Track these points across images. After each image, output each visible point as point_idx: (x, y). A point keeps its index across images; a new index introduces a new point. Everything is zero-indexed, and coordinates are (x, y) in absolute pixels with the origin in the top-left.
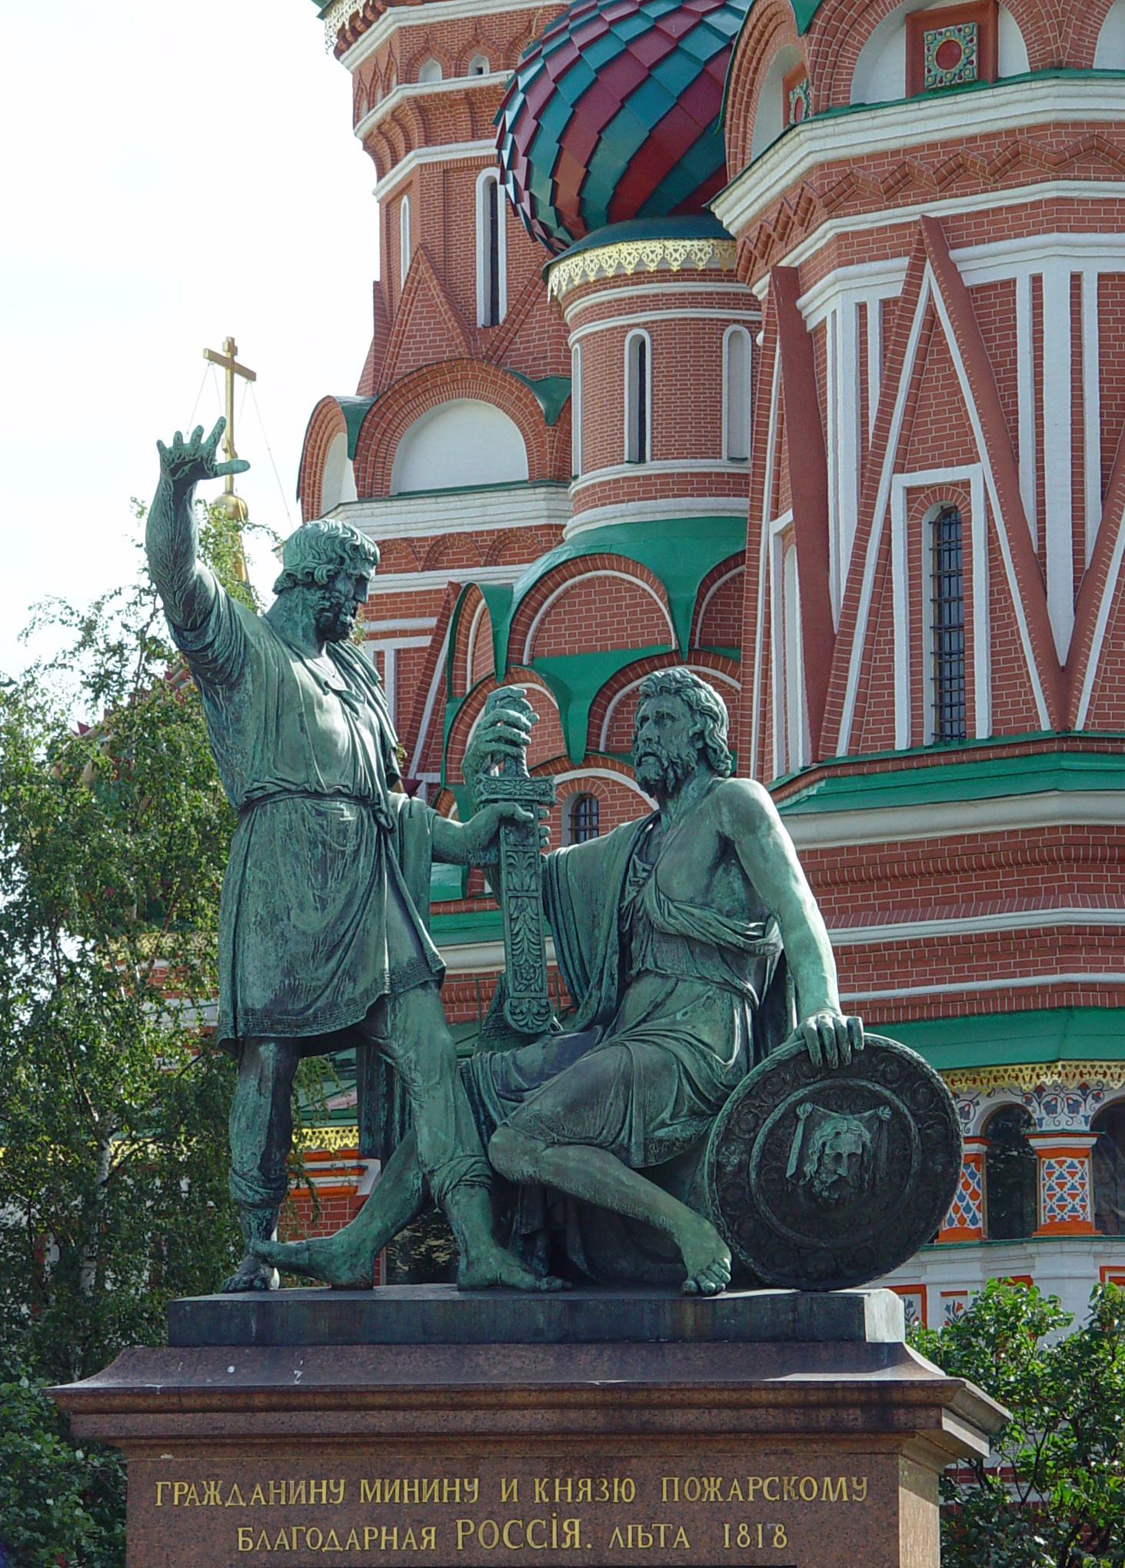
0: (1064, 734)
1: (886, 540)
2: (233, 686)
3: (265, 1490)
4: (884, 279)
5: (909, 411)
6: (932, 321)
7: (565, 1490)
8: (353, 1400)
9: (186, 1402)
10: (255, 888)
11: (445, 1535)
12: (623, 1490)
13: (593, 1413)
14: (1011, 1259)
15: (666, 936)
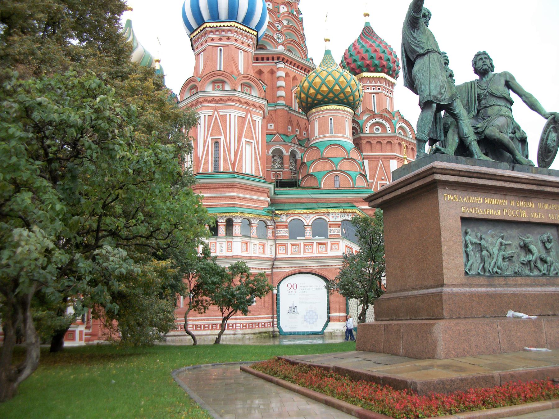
0: (234, 172)
1: (208, 145)
2: (418, 29)
3: (467, 198)
4: (209, 112)
5: (212, 129)
6: (216, 118)
7: (522, 204)
8: (493, 177)
9: (461, 173)
10: (433, 69)
11: (502, 211)
12: (532, 205)
13: (534, 186)
14: (229, 239)
15: (499, 97)
